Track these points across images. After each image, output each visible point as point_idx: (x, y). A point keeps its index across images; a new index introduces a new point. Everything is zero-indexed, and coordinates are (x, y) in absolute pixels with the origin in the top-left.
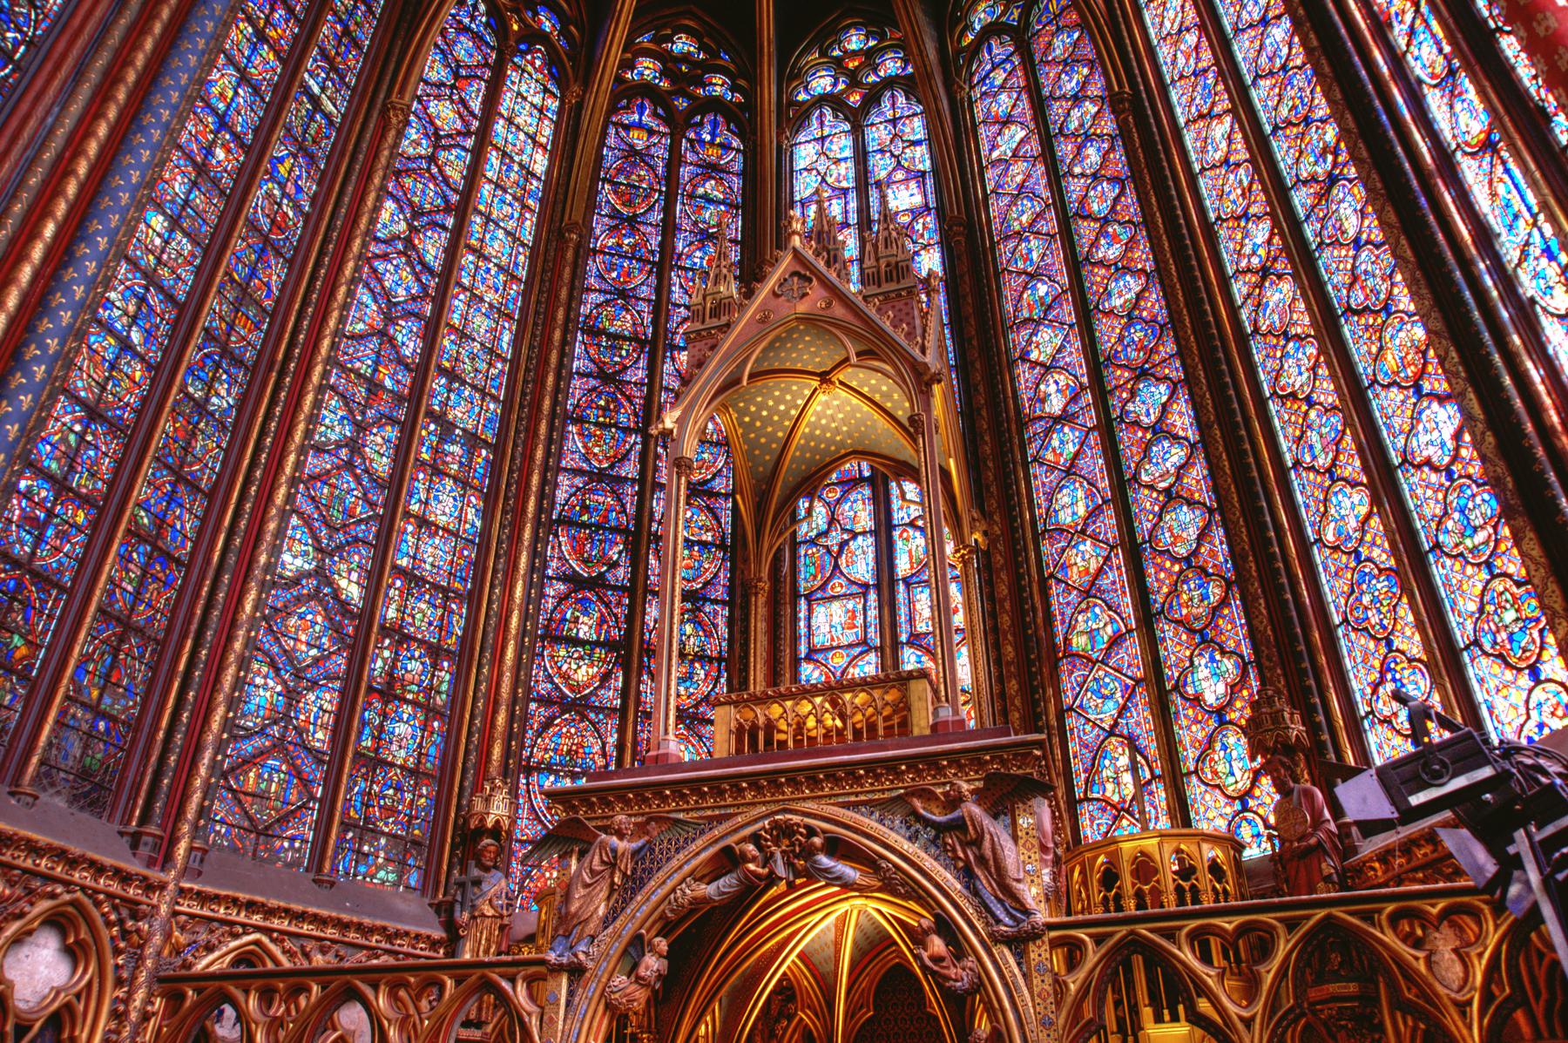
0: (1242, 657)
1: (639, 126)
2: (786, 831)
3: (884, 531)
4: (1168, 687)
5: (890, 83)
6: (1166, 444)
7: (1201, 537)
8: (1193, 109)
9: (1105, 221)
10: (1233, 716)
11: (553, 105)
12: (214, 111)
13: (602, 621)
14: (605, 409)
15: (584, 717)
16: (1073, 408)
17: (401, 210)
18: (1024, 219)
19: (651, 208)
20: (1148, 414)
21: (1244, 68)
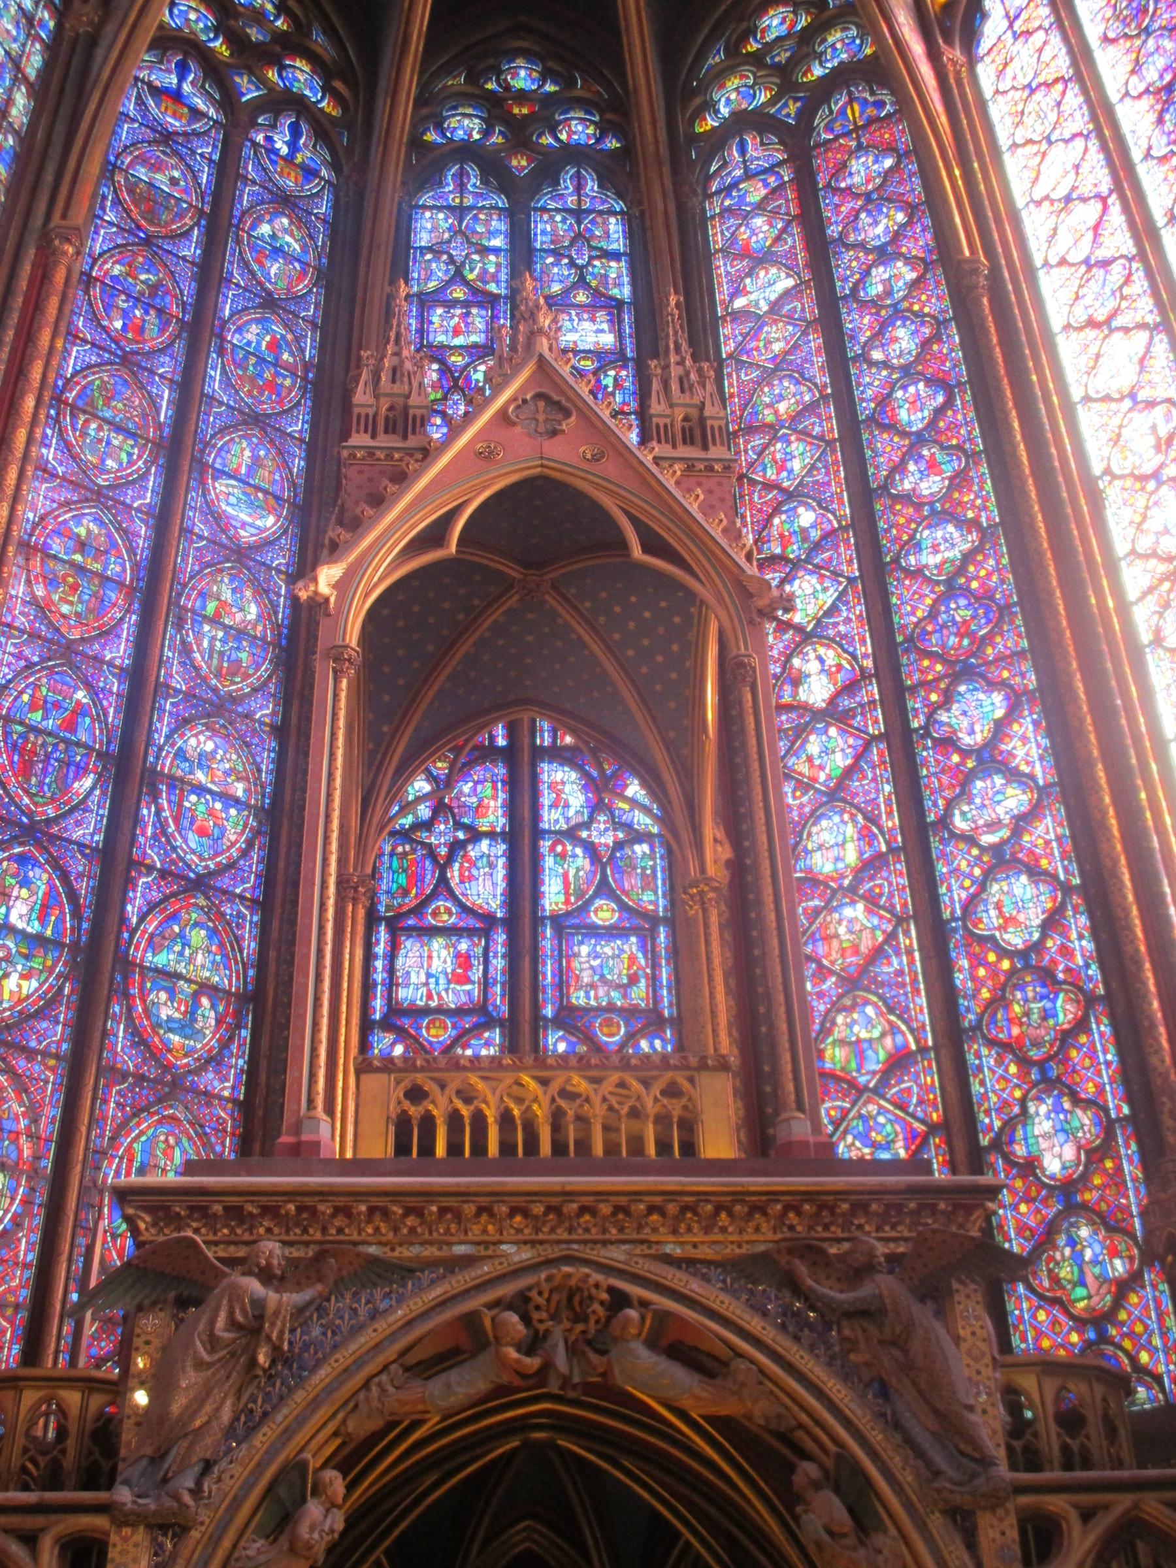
0: (1106, 1110)
2: (573, 1302)
3: (523, 841)
4: (985, 1141)
6: (999, 780)
7: (1053, 922)
9: (919, 439)
10: (1087, 1196)
16: (846, 703)
18: (782, 407)
20: (972, 732)
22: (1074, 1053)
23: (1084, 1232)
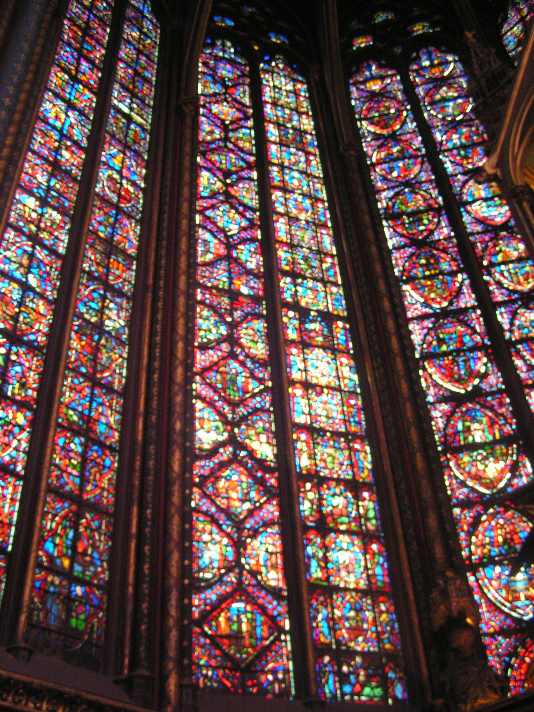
1: (373, 78)
12: (54, 128)
13: (492, 424)
14: (427, 266)
17: (215, 175)
19: (404, 123)
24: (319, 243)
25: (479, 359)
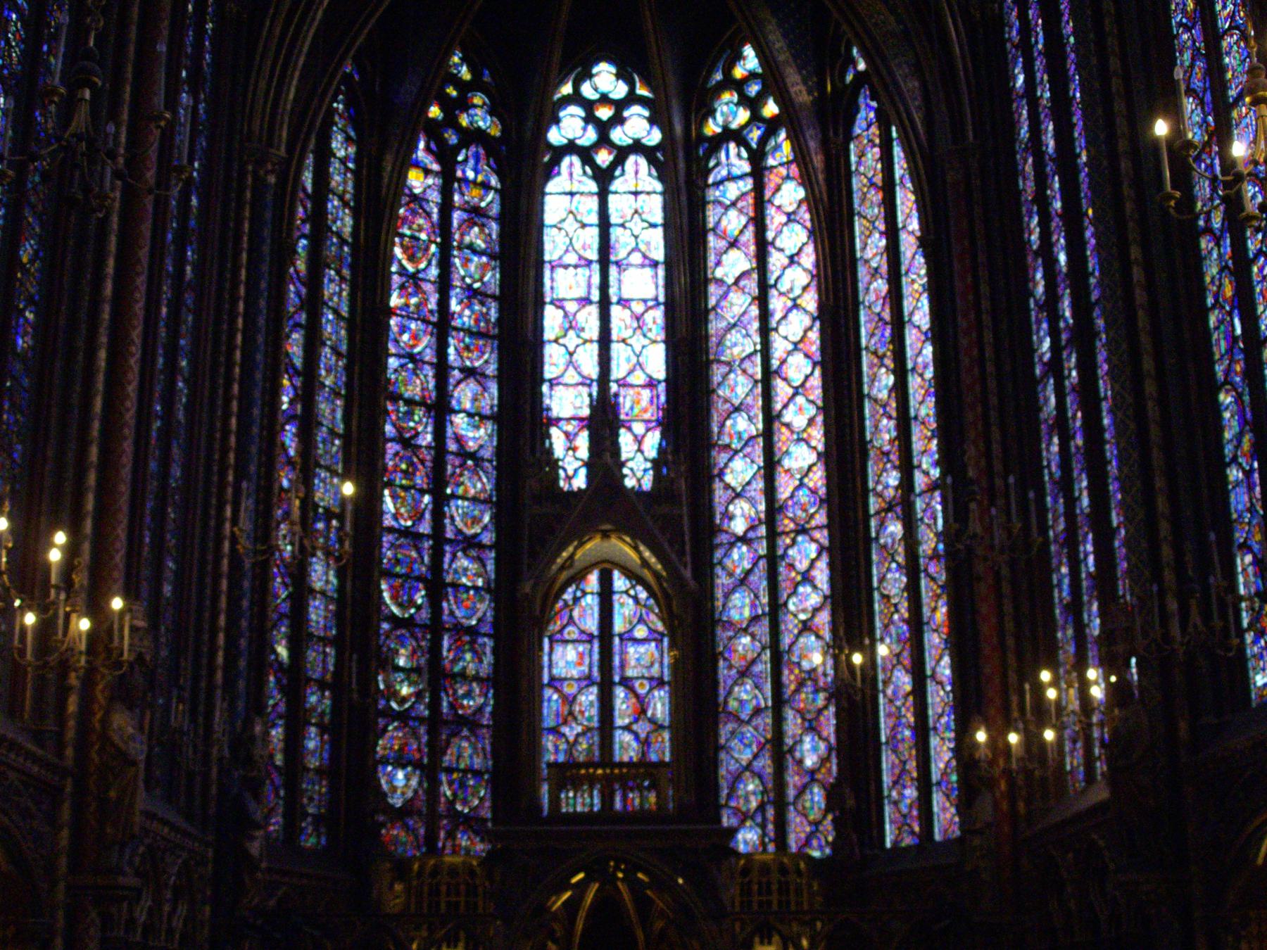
4: (786, 748)
5: (637, 147)
6: (809, 589)
8: (873, 342)
11: (352, 150)
13: (414, 652)
15: (406, 725)
16: (751, 535)
18: (736, 351)
19: (429, 264)
21: (909, 353)
22: (822, 718)
23: (816, 790)
24: (334, 418)
25: (418, 590)
